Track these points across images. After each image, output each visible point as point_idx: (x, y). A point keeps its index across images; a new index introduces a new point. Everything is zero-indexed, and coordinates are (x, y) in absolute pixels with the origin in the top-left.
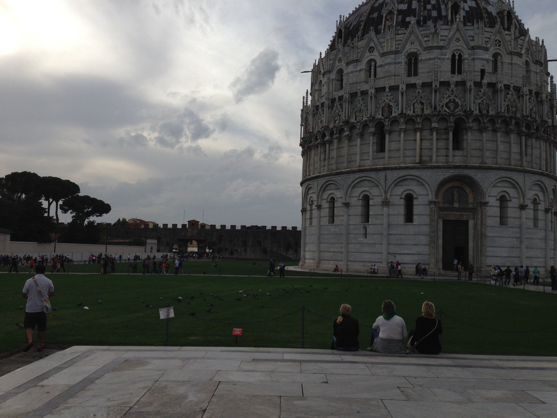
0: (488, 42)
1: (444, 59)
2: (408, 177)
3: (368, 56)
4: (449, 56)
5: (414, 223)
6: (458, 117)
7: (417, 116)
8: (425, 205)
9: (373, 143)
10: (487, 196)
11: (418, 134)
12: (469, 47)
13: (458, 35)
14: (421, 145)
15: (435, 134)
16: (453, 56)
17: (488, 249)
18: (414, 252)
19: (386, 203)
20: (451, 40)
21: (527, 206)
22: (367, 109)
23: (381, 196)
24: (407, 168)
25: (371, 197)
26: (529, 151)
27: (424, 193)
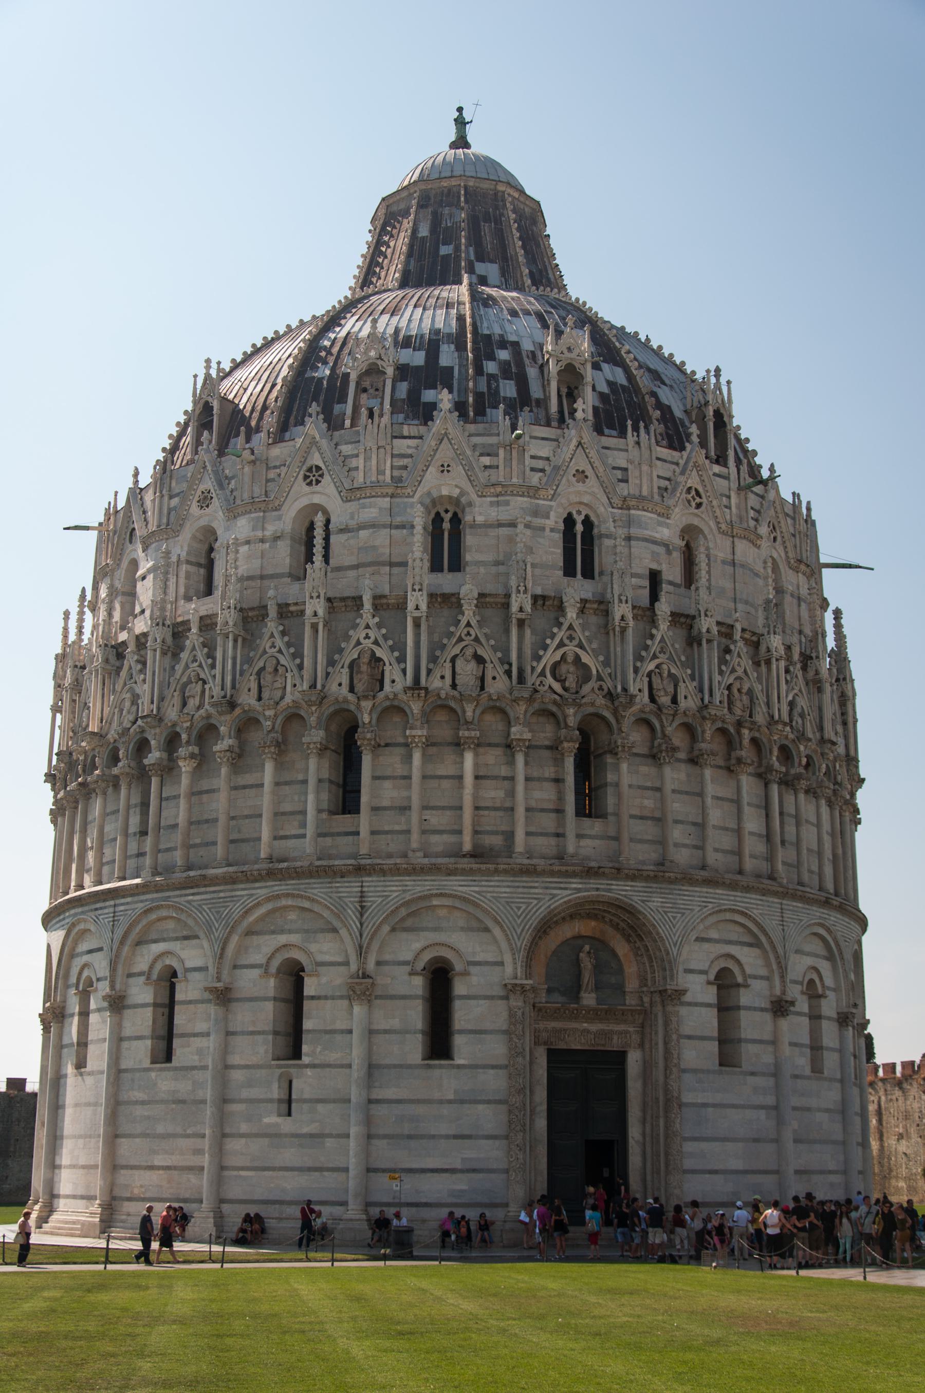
0: (666, 489)
1: (543, 529)
2: (435, 902)
3: (301, 497)
4: (555, 520)
5: (459, 1061)
6: (591, 710)
8: (491, 998)
9: (320, 781)
10: (681, 969)
12: (616, 501)
14: (475, 797)
15: (520, 759)
16: (569, 521)
17: (689, 1147)
18: (459, 1167)
19: (363, 988)
21: (792, 1003)
22: (300, 667)
23: (346, 963)
24: (434, 870)
26: (791, 829)
27: (490, 958)
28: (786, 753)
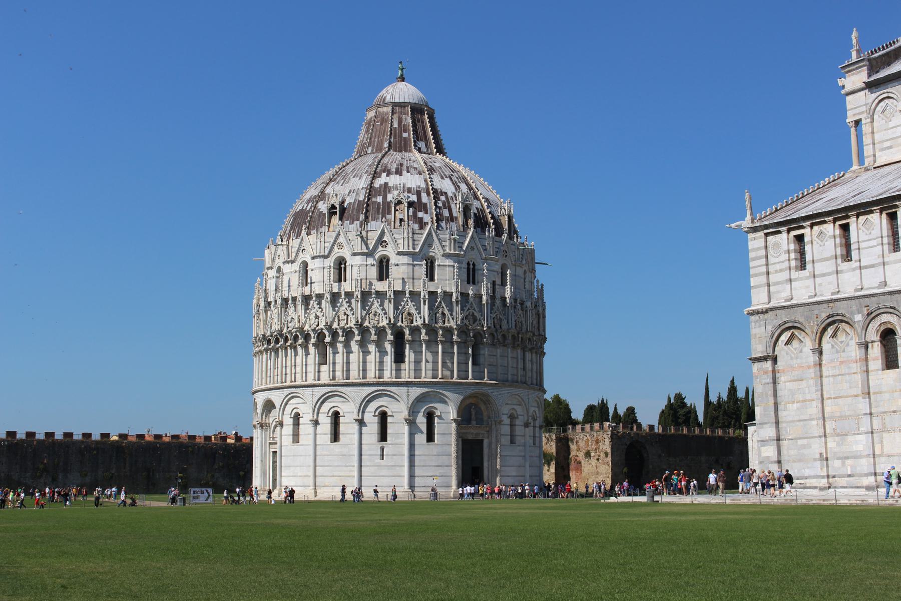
16: (468, 264)
25: (389, 413)
28: (529, 340)
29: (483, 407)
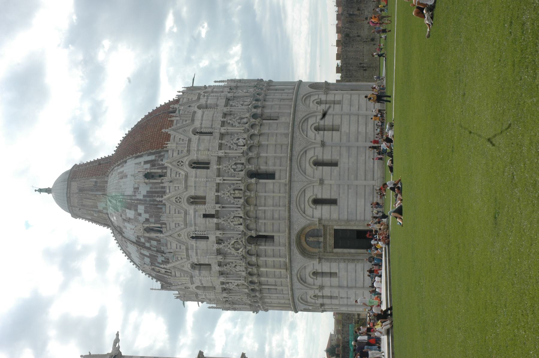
1: (196, 246)
2: (299, 276)
4: (193, 242)
7: (247, 270)
10: (313, 219)
11: (262, 269)
13: (176, 235)
16: (193, 238)
17: (358, 218)
20: (179, 241)
29: (308, 230)
